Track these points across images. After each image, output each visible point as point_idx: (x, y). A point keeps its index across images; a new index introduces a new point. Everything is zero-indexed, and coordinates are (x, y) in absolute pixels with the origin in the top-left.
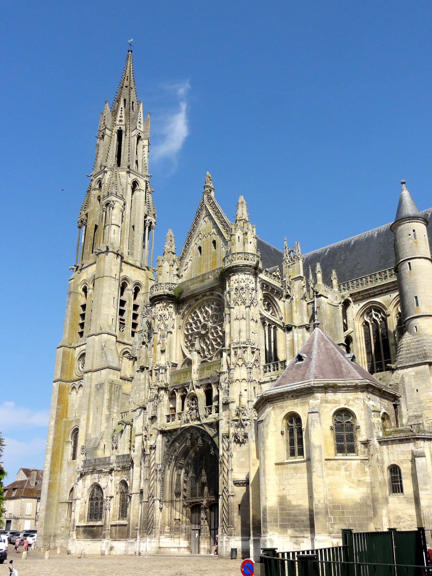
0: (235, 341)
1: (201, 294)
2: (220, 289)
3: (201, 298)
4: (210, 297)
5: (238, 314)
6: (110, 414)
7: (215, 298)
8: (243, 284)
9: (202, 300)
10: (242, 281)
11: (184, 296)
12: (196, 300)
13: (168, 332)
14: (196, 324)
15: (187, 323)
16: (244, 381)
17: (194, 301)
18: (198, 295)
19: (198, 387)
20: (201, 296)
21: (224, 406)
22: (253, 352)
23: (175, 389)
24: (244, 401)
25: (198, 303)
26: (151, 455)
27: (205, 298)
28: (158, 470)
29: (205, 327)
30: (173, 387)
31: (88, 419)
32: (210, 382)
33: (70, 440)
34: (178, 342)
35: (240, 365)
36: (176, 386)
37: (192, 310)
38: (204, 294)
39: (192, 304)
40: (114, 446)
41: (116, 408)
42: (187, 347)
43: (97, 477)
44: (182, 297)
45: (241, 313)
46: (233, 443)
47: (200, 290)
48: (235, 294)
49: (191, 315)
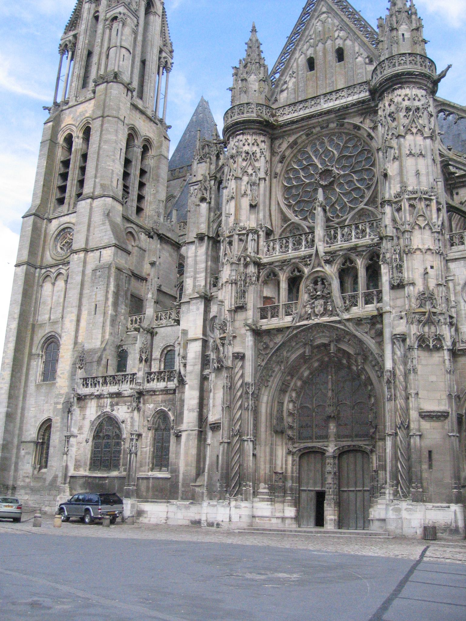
0: (410, 188)
5: (413, 147)
6: (116, 315)
8: (417, 104)
10: (417, 99)
13: (260, 179)
16: (429, 252)
19: (327, 262)
21: (391, 291)
22: (439, 210)
24: (432, 284)
26: (236, 370)
28: (250, 393)
29: (327, 173)
31: (78, 321)
33: (41, 353)
35: (422, 225)
40: (144, 358)
41: (124, 307)
45: (418, 147)
46: (416, 351)
48: (405, 116)
49: (296, 157)
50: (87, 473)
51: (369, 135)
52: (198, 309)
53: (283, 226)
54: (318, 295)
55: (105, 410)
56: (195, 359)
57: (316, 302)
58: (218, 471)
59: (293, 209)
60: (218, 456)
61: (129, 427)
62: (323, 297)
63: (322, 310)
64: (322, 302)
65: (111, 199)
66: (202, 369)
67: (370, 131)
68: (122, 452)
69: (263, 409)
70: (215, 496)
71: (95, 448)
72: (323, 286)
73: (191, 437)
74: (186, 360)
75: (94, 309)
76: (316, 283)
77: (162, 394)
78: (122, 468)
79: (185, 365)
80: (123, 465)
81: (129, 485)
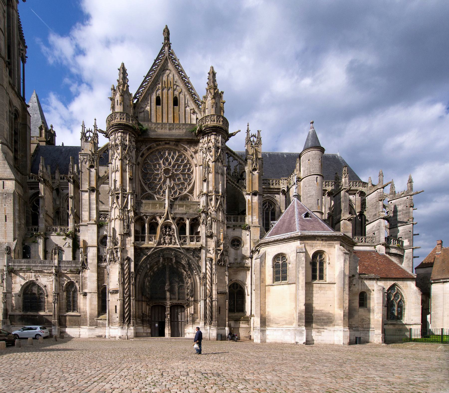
1: (165, 141)
3: (164, 145)
9: (164, 147)
20: (163, 143)
23: (145, 215)
27: (167, 146)
34: (137, 176)
36: (146, 213)
43: (33, 276)
50: (22, 313)
51: (191, 156)
52: (93, 230)
53: (142, 194)
54: (168, 234)
55: (31, 280)
58: (116, 312)
59: (148, 186)
60: (116, 306)
61: (50, 289)
62: (169, 235)
63: (169, 241)
64: (169, 237)
65: (6, 147)
66: (98, 262)
67: (193, 154)
68: (46, 302)
69: (137, 286)
70: (116, 324)
71: (25, 299)
72: (170, 230)
73: (93, 296)
74: (87, 256)
75: (4, 218)
76: (166, 227)
77: (70, 273)
78: (47, 311)
79: (86, 260)
80: (48, 309)
81: (55, 319)
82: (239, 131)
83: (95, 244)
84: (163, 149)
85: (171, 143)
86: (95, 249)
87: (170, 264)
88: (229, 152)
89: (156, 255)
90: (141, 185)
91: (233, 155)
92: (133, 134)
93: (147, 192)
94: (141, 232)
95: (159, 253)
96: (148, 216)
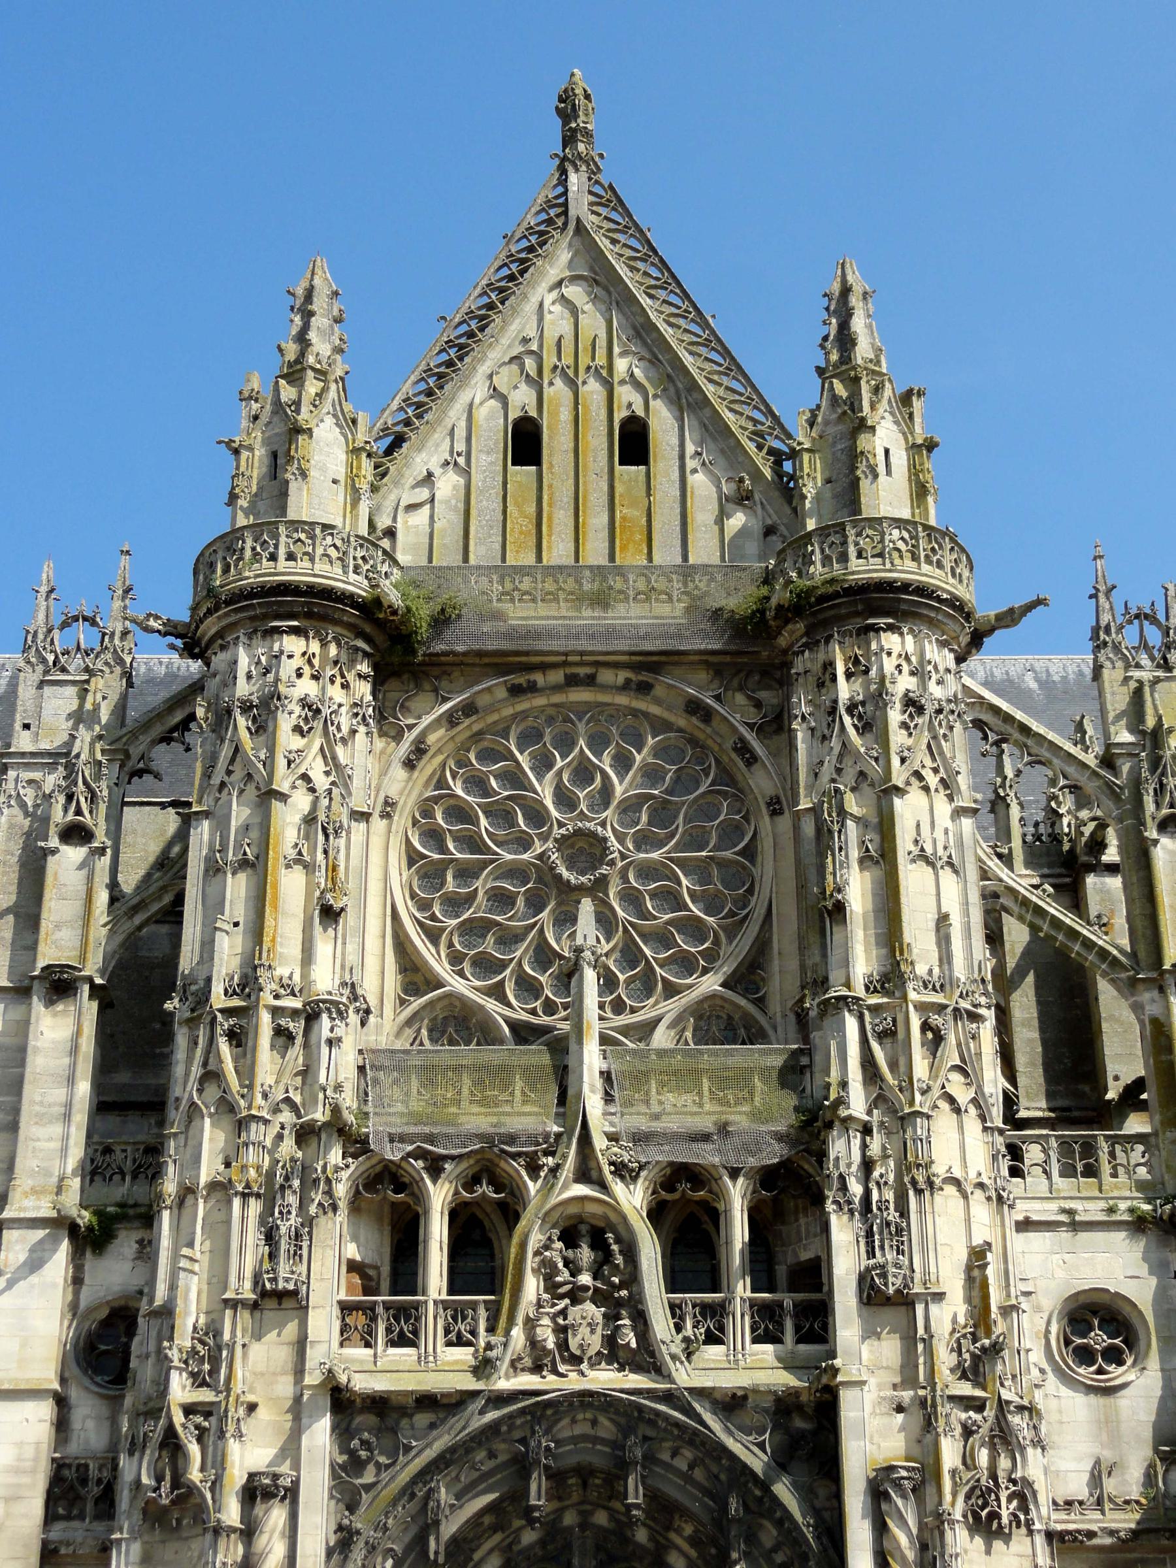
1: (565, 664)
2: (703, 676)
3: (556, 688)
4: (622, 700)
7: (655, 710)
9: (557, 698)
11: (456, 642)
12: (516, 691)
14: (501, 814)
15: (436, 800)
17: (502, 693)
18: (543, 667)
19: (621, 1170)
20: (557, 677)
23: (419, 1154)
25: (523, 705)
30: (403, 1139)
32: (708, 1156)
36: (431, 1139)
37: (478, 736)
38: (583, 671)
39: (483, 701)
42: (433, 936)
44: (440, 647)
47: (584, 645)
56: (17, 1471)
57: (575, 1312)
82: (1040, 602)
83: (47, 1374)
84: (551, 711)
85: (606, 676)
86: (45, 1410)
87: (601, 1518)
88: (986, 717)
89: (492, 1455)
90: (402, 946)
91: (1016, 735)
92: (360, 634)
93: (440, 984)
94: (386, 1270)
95: (517, 1435)
96: (445, 1158)
